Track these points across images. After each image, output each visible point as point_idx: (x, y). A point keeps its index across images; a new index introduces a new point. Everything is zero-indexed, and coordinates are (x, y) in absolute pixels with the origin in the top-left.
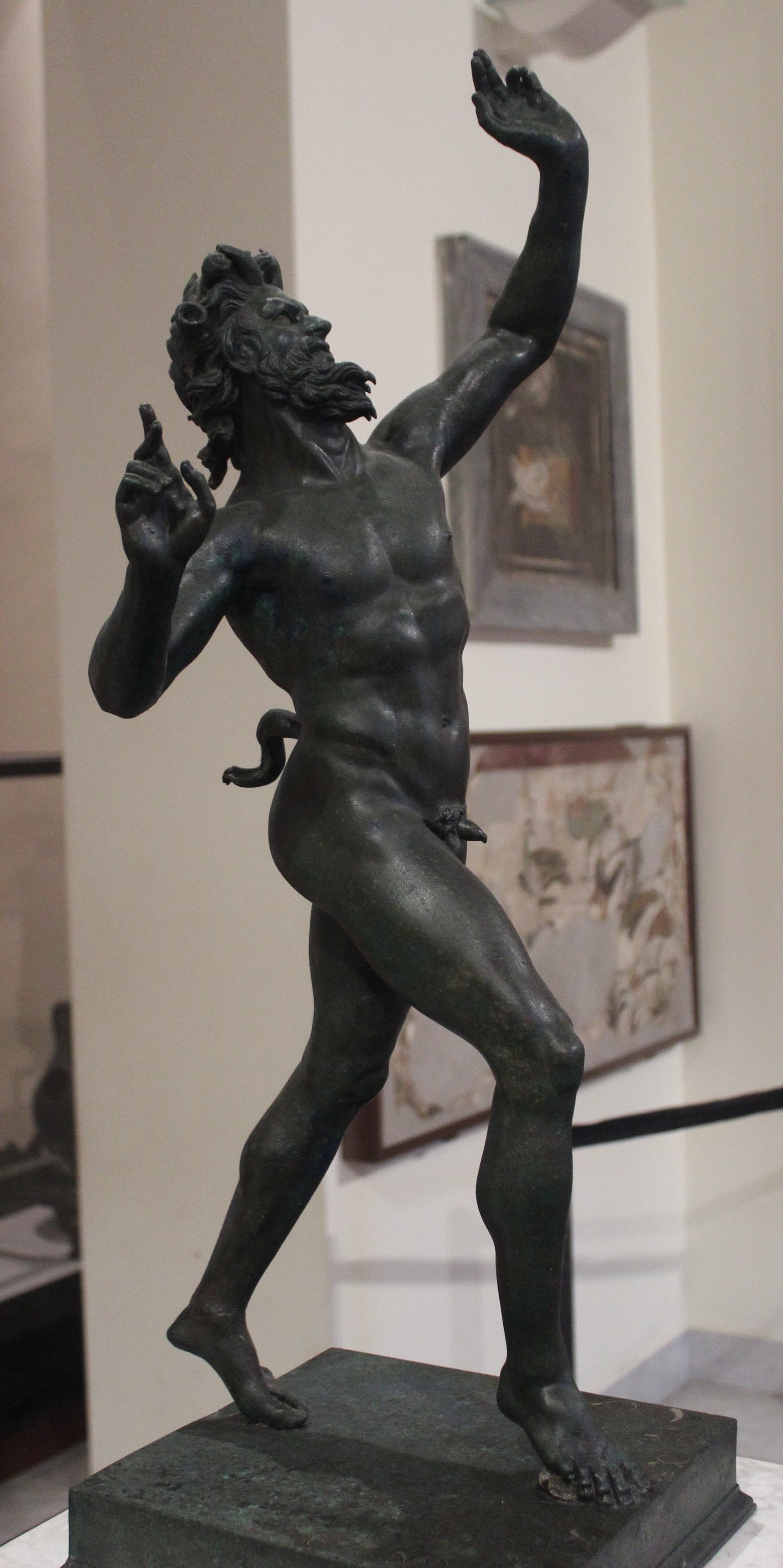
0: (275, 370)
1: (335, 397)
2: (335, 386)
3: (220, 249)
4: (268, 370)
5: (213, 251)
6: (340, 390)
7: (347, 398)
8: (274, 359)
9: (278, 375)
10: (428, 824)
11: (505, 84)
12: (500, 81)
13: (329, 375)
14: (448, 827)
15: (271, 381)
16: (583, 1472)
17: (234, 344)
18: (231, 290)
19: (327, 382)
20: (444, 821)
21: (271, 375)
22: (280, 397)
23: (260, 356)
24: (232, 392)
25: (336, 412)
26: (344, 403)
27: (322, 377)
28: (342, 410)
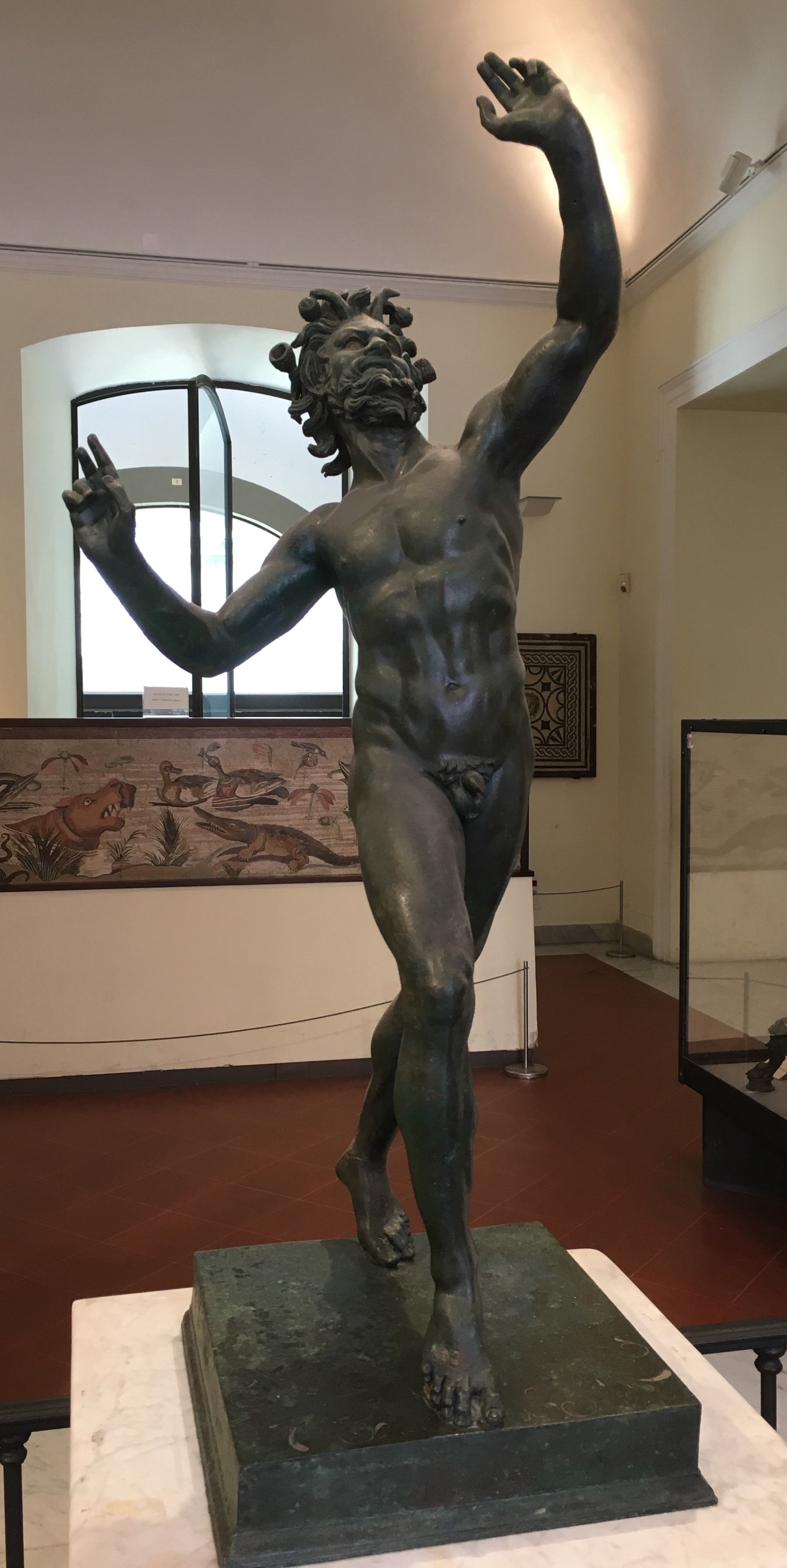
0: (332, 390)
1: (365, 406)
2: (366, 397)
3: (316, 295)
4: (329, 391)
6: (369, 400)
10: (430, 774)
14: (451, 778)
15: (332, 400)
16: (438, 1379)
17: (311, 373)
18: (318, 326)
20: (445, 771)
22: (338, 412)
24: (323, 413)
25: (373, 419)
27: (358, 391)
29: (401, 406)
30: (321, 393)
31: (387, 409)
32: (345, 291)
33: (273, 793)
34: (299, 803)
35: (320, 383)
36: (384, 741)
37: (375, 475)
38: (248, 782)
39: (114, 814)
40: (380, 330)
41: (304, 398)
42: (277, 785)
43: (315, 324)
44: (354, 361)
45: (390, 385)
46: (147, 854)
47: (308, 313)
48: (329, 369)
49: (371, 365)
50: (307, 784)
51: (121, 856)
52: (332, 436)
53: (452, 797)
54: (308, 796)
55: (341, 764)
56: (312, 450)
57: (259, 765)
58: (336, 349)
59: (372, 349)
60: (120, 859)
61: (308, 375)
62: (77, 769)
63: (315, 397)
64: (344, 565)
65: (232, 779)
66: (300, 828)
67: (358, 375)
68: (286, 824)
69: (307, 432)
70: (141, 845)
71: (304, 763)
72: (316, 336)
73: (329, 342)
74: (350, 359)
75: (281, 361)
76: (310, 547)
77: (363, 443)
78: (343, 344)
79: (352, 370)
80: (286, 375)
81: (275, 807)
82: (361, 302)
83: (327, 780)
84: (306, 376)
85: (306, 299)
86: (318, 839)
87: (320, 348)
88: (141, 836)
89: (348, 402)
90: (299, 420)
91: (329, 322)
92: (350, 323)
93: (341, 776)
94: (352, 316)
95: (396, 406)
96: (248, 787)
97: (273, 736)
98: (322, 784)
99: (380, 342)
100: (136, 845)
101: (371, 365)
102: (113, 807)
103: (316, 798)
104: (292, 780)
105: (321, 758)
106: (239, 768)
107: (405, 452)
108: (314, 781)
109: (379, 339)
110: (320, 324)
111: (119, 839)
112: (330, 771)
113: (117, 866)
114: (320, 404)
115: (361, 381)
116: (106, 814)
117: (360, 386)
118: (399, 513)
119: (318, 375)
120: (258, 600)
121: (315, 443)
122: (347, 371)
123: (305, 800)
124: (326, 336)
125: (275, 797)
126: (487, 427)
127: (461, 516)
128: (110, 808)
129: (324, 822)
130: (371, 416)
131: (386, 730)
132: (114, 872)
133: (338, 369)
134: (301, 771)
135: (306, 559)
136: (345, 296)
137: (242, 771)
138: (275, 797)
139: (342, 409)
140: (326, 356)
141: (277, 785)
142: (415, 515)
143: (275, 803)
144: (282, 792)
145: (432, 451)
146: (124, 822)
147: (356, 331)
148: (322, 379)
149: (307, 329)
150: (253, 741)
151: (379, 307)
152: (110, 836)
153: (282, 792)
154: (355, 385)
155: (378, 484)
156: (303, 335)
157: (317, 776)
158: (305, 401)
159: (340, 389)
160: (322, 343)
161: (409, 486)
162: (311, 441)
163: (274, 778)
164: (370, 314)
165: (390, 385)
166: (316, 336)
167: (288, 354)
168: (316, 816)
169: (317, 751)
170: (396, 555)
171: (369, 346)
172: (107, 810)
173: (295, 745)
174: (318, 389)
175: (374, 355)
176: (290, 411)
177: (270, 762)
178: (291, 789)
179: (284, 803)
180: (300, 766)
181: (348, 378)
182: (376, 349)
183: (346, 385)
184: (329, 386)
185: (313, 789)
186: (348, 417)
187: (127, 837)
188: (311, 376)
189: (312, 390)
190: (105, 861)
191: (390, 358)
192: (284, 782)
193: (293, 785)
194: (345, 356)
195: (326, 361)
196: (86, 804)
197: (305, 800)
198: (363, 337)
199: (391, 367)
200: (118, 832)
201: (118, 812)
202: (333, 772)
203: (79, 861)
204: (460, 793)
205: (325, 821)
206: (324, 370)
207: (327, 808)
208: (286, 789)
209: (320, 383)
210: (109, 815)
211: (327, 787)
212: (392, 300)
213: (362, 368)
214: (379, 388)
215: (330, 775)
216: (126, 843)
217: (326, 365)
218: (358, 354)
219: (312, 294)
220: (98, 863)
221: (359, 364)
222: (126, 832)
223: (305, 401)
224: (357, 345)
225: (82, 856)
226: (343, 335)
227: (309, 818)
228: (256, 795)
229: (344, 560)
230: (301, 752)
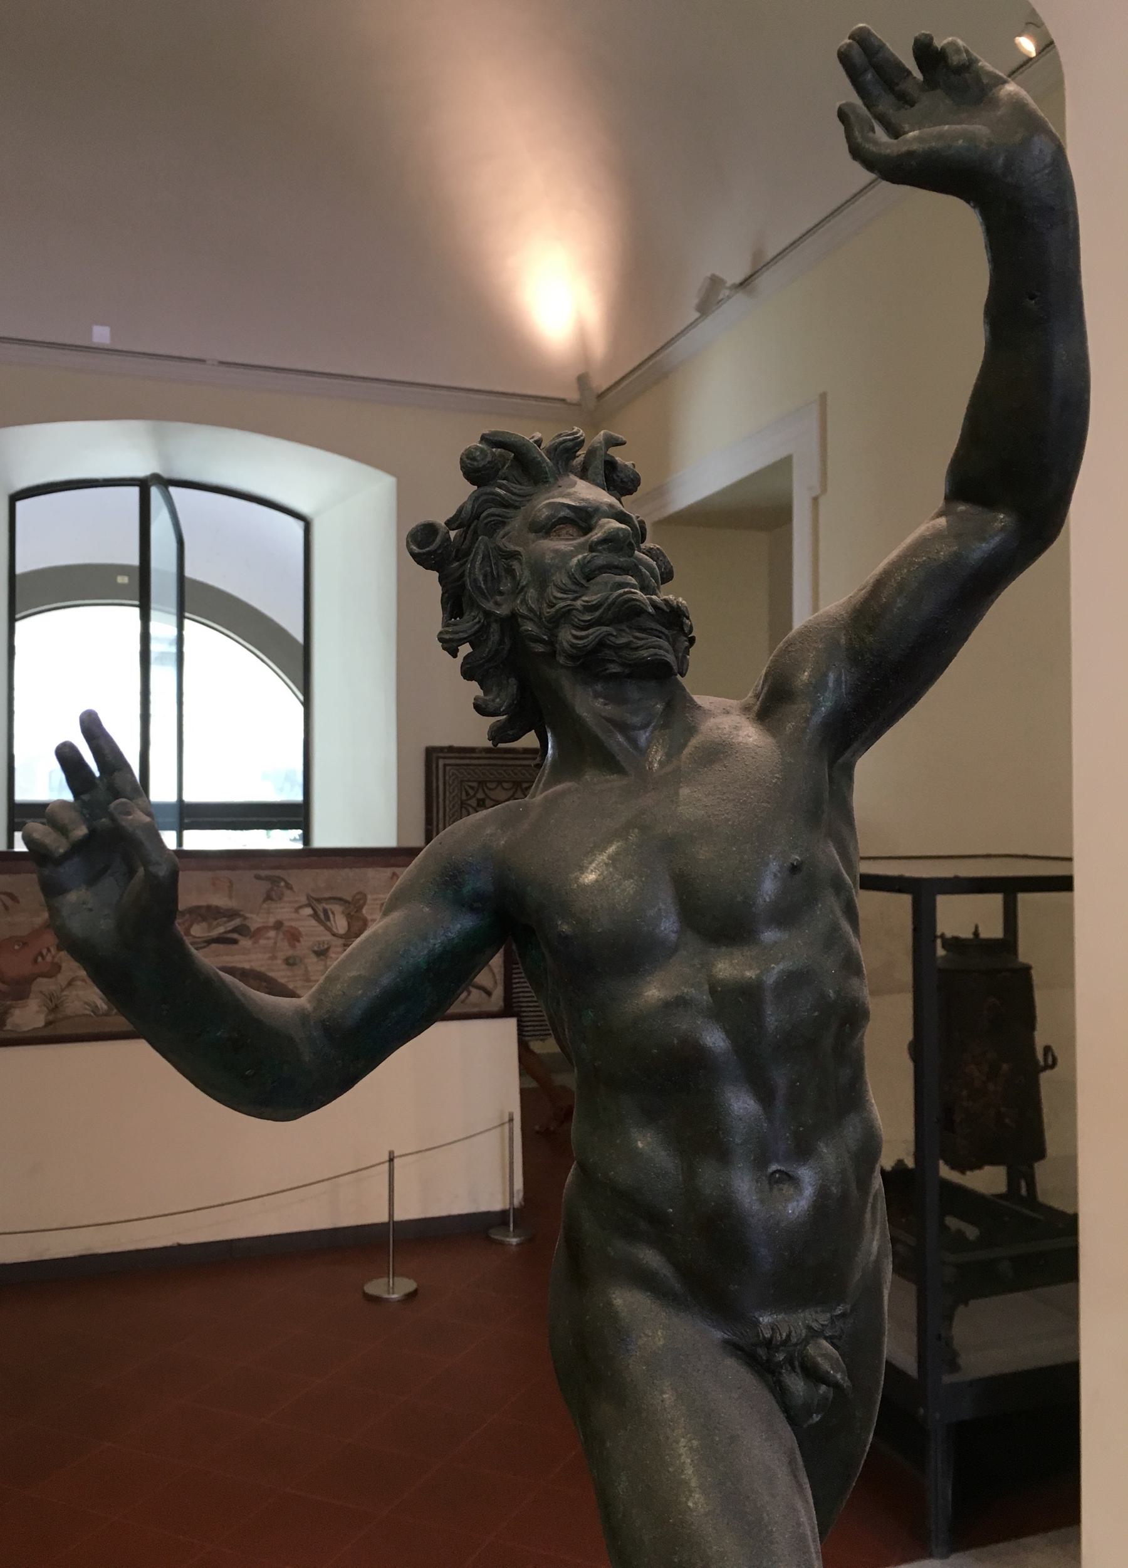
0: (531, 610)
1: (601, 644)
2: (605, 629)
4: (523, 610)
5: (476, 442)
7: (627, 645)
8: (532, 593)
9: (537, 618)
11: (917, 74)
12: (909, 73)
13: (597, 614)
14: (781, 1357)
15: (529, 627)
17: (485, 576)
19: (598, 622)
20: (768, 1344)
21: (531, 620)
22: (540, 648)
23: (518, 590)
24: (501, 642)
25: (614, 668)
26: (624, 653)
28: (623, 665)
29: (670, 648)
30: (503, 611)
31: (645, 653)
32: (538, 435)
33: (233, 931)
34: (262, 942)
35: (501, 593)
36: (645, 1280)
37: (609, 763)
38: (204, 919)
39: (49, 958)
40: (611, 506)
41: (466, 617)
42: (237, 922)
43: (488, 489)
44: (575, 561)
45: (650, 610)
46: (86, 1003)
47: (475, 471)
48: (524, 575)
49: (603, 569)
50: (272, 920)
51: (56, 1007)
52: (512, 681)
53: (781, 1393)
54: (272, 934)
55: (309, 897)
56: (481, 709)
57: (219, 900)
58: (532, 536)
59: (604, 541)
60: (55, 1009)
61: (481, 578)
62: (6, 908)
63: (488, 614)
64: (564, 938)
65: (187, 916)
66: (263, 969)
67: (582, 586)
68: (247, 966)
69: (469, 672)
70: (81, 993)
71: (268, 898)
72: (493, 510)
73: (517, 522)
74: (566, 556)
75: (429, 553)
76: (480, 882)
77: (588, 705)
78: (547, 528)
79: (571, 577)
80: (435, 575)
81: (235, 947)
82: (565, 452)
83: (294, 916)
84: (475, 580)
85: (477, 448)
86: (283, 981)
87: (502, 533)
88: (79, 983)
89: (567, 636)
90: (454, 654)
91: (516, 488)
92: (556, 492)
93: (309, 911)
94: (556, 479)
95: (658, 647)
96: (204, 925)
97: (233, 869)
98: (290, 920)
99: (619, 529)
100: (74, 993)
101: (603, 569)
102: (49, 950)
103: (281, 936)
104: (254, 916)
105: (288, 892)
106: (195, 903)
107: (665, 726)
108: (279, 917)
109: (615, 524)
110: (499, 490)
111: (53, 987)
112: (296, 905)
113: (51, 1018)
114: (495, 627)
115: (591, 598)
116: (40, 959)
117: (589, 608)
118: (670, 846)
119: (497, 579)
120: (385, 981)
121: (481, 693)
122: (561, 578)
123: (268, 938)
124: (510, 512)
125: (235, 936)
126: (819, 684)
127: (796, 857)
128: (44, 952)
129: (290, 962)
130: (613, 661)
131: (650, 1258)
132: (48, 1024)
133: (542, 575)
134: (265, 906)
135: (473, 904)
136: (539, 442)
137: (199, 907)
138: (235, 936)
139: (551, 643)
140: (512, 547)
141: (237, 922)
142: (703, 853)
143: (235, 942)
144: (242, 930)
145: (711, 722)
146: (60, 967)
147: (569, 507)
148: (506, 586)
149: (475, 498)
150: (210, 874)
151: (598, 464)
152: (44, 985)
153: (242, 930)
154: (579, 603)
155: (616, 782)
156: (469, 507)
157: (283, 912)
158: (468, 623)
159: (548, 612)
160: (504, 524)
161: (684, 791)
162: (474, 689)
163: (232, 914)
164: (583, 474)
165: (650, 610)
166: (493, 510)
167: (443, 542)
168: (281, 955)
169: (282, 884)
170: (669, 926)
171: (596, 535)
172: (41, 954)
173: (258, 877)
174: (497, 604)
175: (610, 551)
176: (441, 640)
177: (230, 897)
178: (253, 927)
179: (245, 943)
180: (265, 901)
181: (564, 592)
182: (611, 541)
183: (562, 604)
184: (524, 601)
185: (278, 925)
186: (561, 660)
187: (64, 983)
188: (485, 581)
189: (488, 606)
190: (38, 1012)
191: (632, 555)
192: (245, 918)
193: (256, 921)
194: (556, 551)
195: (514, 555)
196: (16, 947)
197: (268, 938)
198: (582, 518)
199: (633, 569)
200: (53, 980)
201: (53, 957)
202: (301, 907)
203: (6, 1012)
204: (797, 1385)
205: (291, 961)
206: (510, 571)
207: (293, 946)
208: (248, 928)
209: (501, 593)
210: (43, 958)
211: (293, 924)
212: (612, 451)
213: (589, 573)
214: (627, 613)
215: (297, 910)
216: (62, 990)
217: (515, 565)
218: (579, 549)
219: (484, 438)
220: (29, 1015)
221: (582, 565)
222: (62, 979)
223: (468, 623)
224: (572, 530)
225: (10, 1007)
226: (546, 513)
227: (274, 958)
228: (215, 933)
229: (565, 928)
230: (265, 886)
